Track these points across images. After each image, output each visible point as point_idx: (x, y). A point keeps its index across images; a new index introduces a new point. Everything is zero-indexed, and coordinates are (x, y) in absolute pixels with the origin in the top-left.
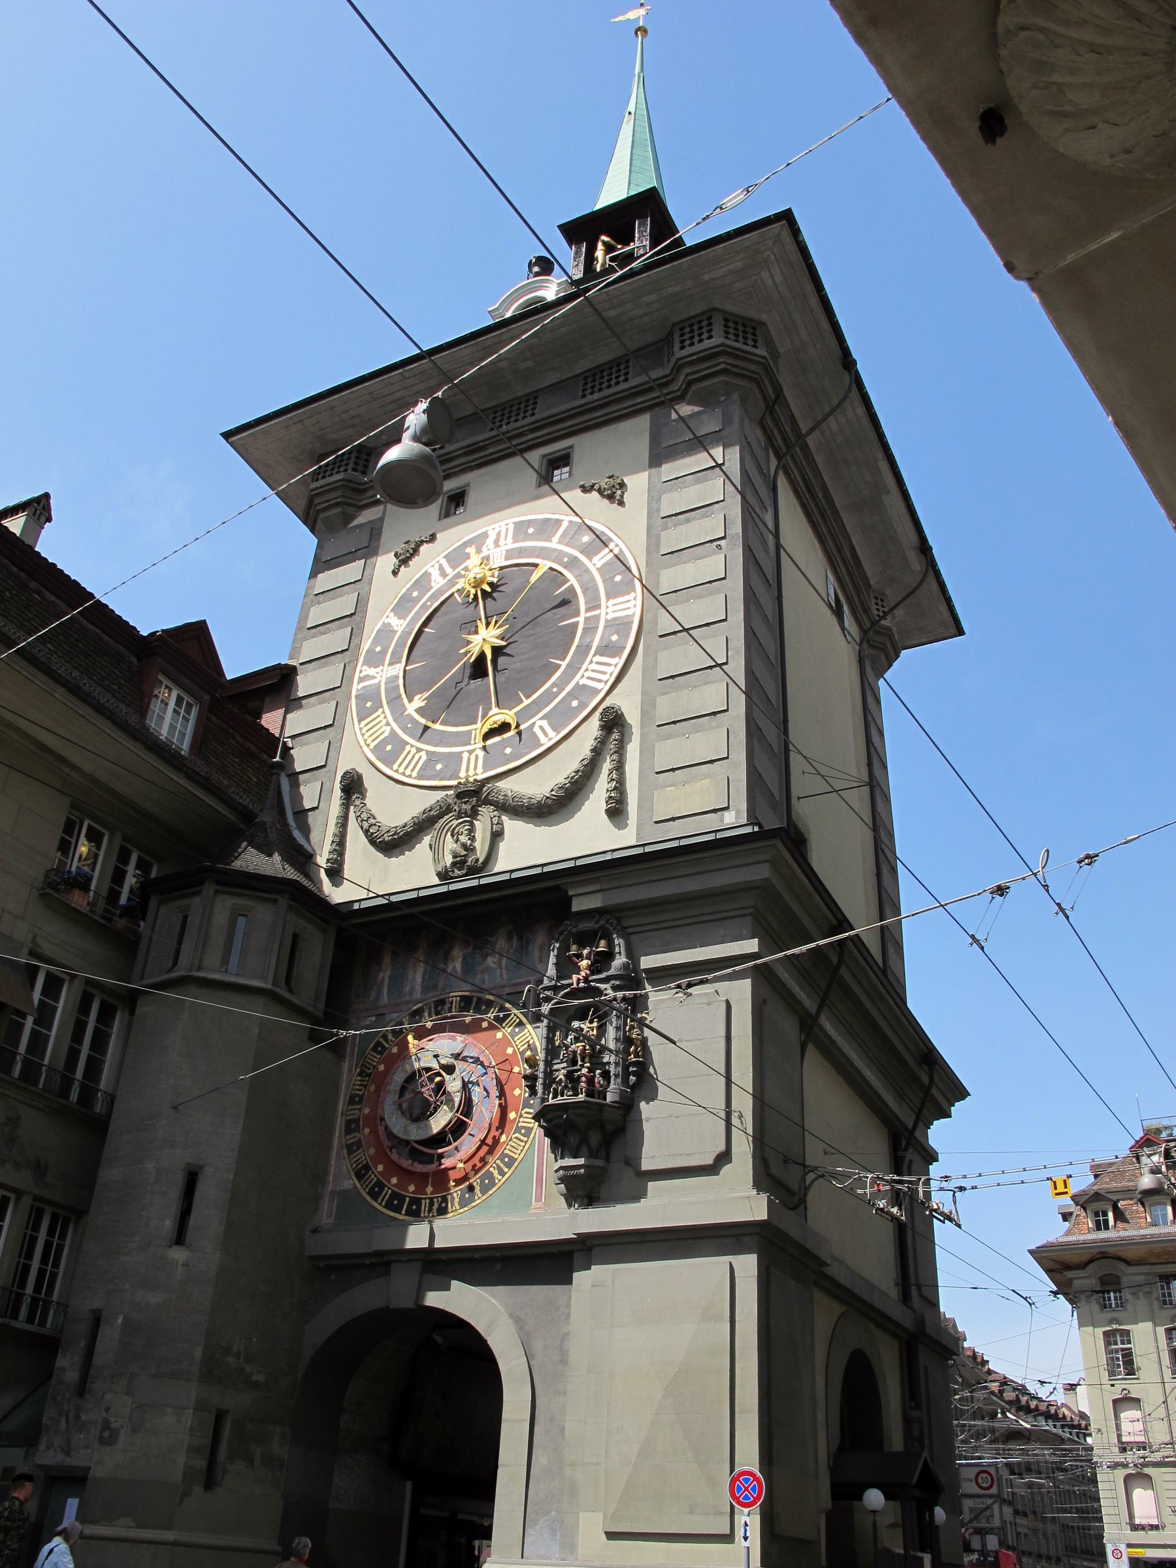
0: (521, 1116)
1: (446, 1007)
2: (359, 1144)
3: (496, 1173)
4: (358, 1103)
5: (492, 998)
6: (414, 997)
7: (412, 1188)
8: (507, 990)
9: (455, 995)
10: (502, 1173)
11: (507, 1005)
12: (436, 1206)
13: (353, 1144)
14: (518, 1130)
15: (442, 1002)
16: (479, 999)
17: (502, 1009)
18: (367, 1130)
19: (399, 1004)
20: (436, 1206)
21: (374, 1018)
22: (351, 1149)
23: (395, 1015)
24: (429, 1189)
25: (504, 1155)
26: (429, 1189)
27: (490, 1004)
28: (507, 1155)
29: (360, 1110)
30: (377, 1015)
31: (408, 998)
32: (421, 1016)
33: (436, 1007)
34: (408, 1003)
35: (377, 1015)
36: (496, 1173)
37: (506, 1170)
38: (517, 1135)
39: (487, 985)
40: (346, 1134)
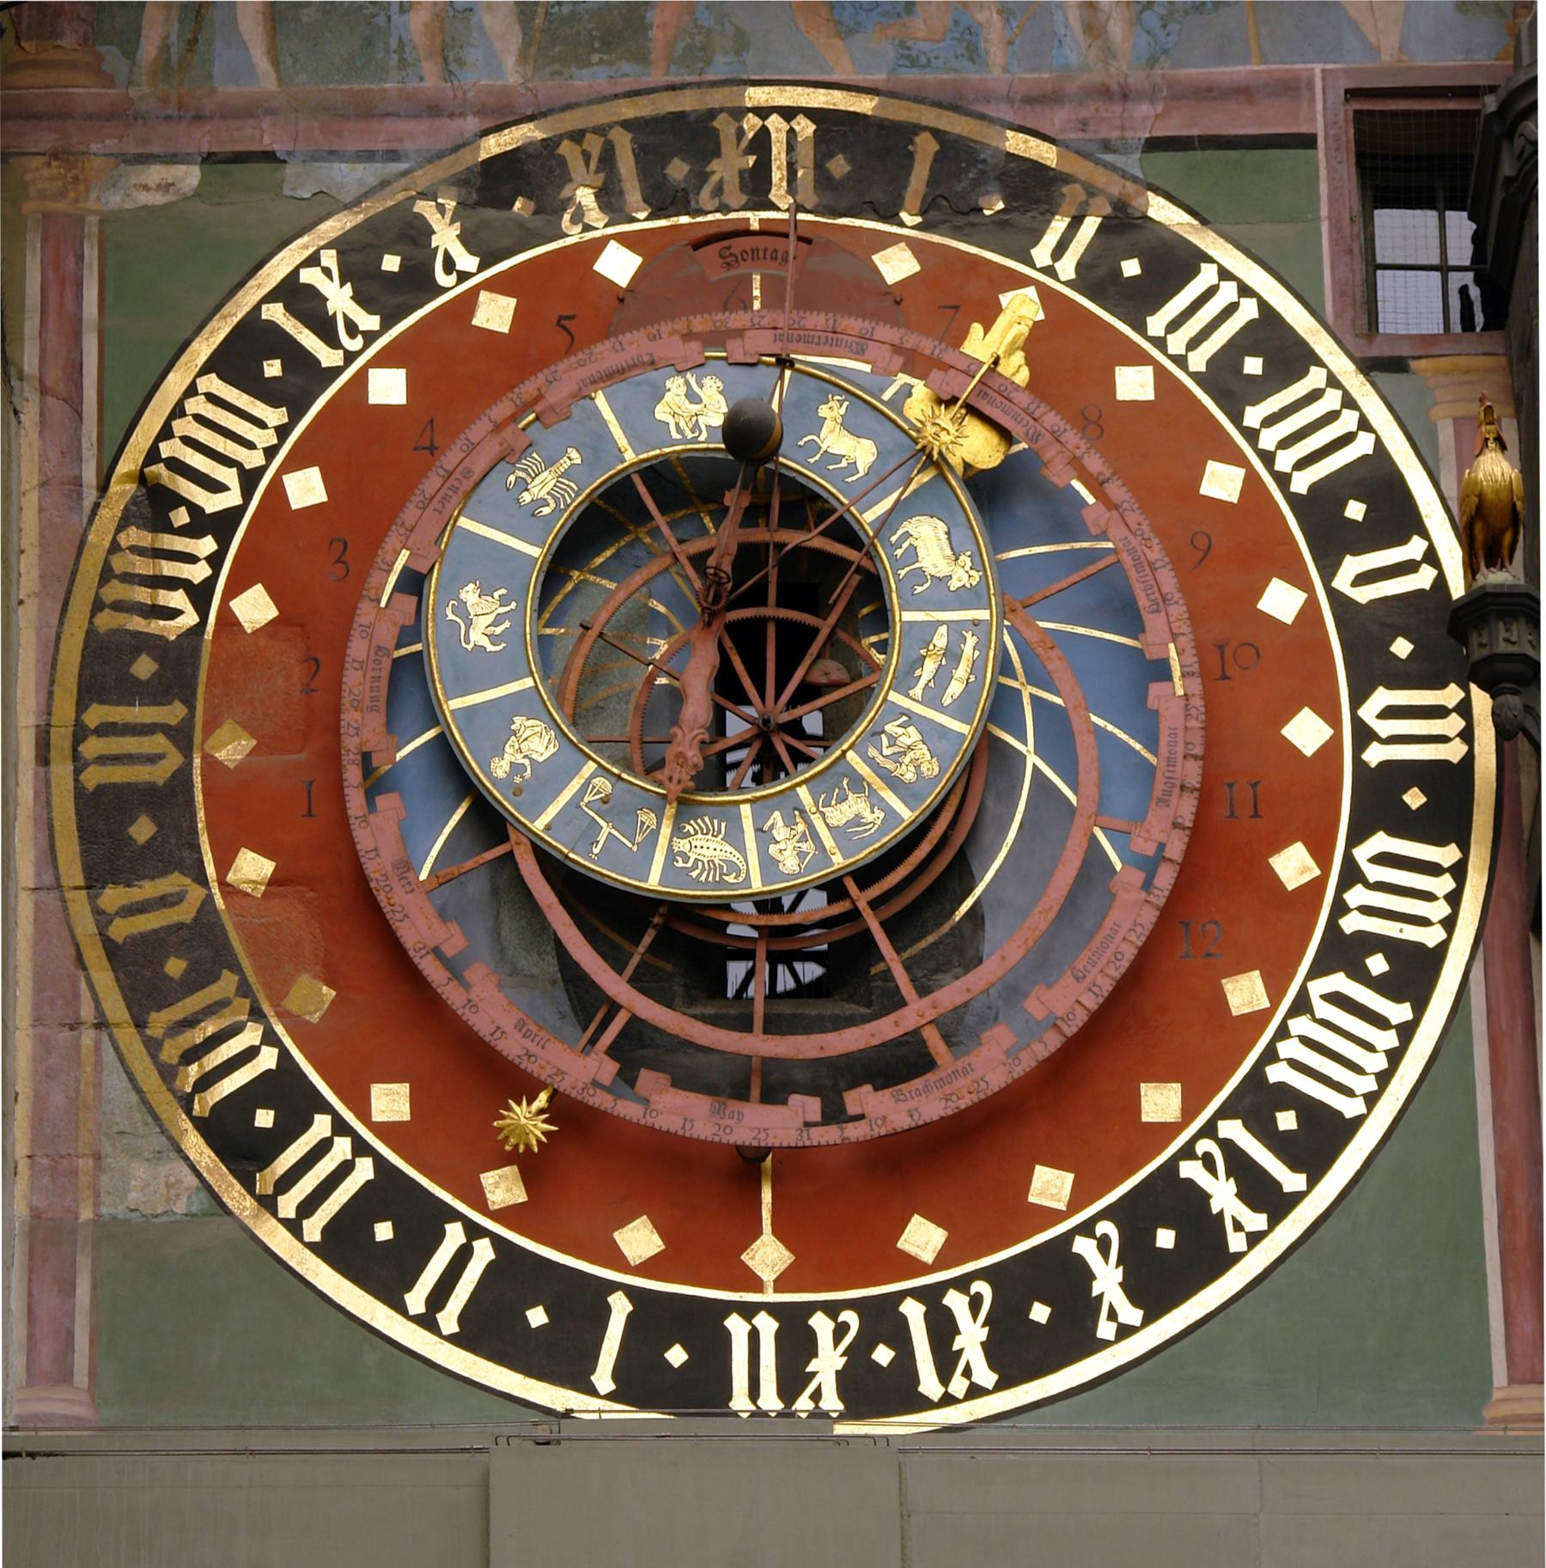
0: (1352, 875)
1: (730, 165)
2: (205, 944)
3: (1223, 1195)
4: (155, 692)
5: (1047, 154)
6: (474, 79)
7: (639, 1240)
8: (1147, 119)
9: (783, 105)
10: (1277, 1204)
11: (1161, 211)
12: (828, 1363)
13: (154, 945)
14: (1344, 952)
15: (693, 136)
16: (956, 155)
17: (1124, 225)
18: (253, 868)
19: (368, 111)
20: (828, 1363)
21: (190, 176)
22: (141, 972)
23: (348, 176)
24: (768, 1256)
25: (1257, 1104)
26: (768, 1256)
27: (1034, 192)
28: (1287, 1096)
29: (181, 736)
30: (209, 159)
31: (429, 79)
32: (551, 207)
33: (650, 161)
34: (434, 110)
35: (209, 159)
36: (1223, 1195)
37: (1292, 1181)
38: (1338, 982)
39: (999, 67)
40: (94, 882)
